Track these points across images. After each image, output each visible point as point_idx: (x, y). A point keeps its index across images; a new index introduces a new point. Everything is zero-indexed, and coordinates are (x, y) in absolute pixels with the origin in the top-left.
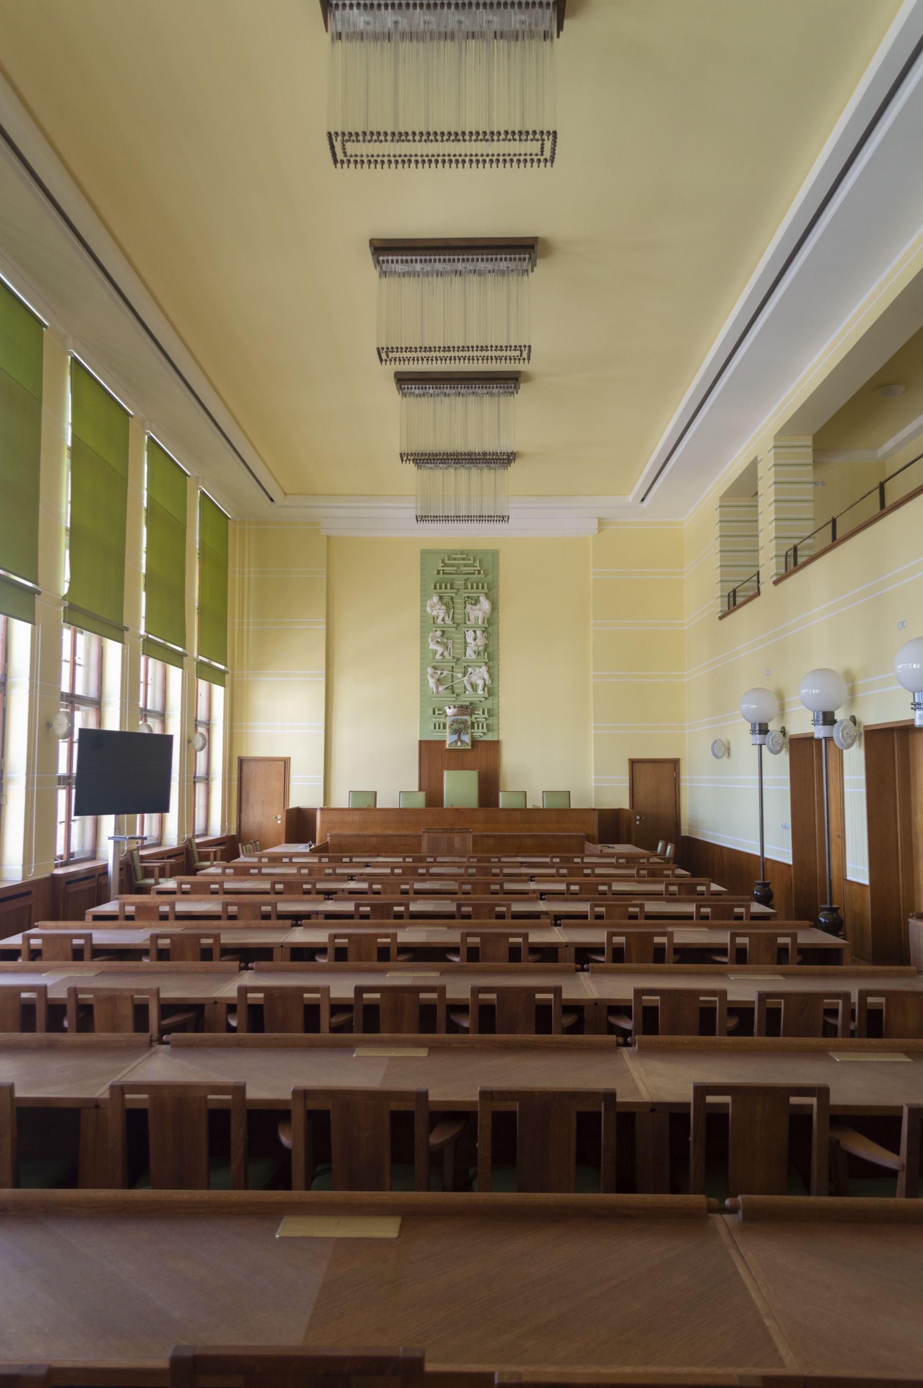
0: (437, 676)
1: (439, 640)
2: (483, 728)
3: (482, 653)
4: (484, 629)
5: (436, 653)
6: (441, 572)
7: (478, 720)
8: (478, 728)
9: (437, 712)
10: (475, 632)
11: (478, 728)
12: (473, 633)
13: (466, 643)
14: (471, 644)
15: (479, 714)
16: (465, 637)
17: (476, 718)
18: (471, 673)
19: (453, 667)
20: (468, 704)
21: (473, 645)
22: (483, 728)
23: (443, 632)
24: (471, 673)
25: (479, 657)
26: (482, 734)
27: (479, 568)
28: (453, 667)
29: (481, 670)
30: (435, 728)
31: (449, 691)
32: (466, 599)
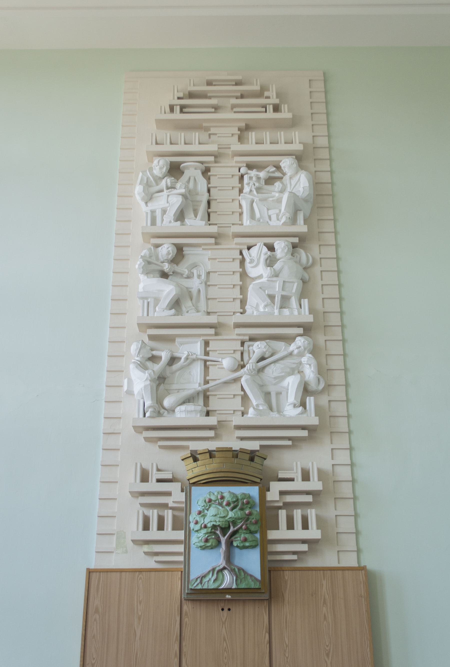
0: (157, 367)
1: (166, 267)
2: (305, 526)
3: (294, 302)
4: (296, 240)
5: (157, 301)
6: (178, 109)
7: (289, 499)
8: (290, 526)
9: (154, 475)
10: (271, 248)
11: (290, 526)
12: (265, 249)
13: (244, 275)
14: (260, 277)
15: (292, 480)
16: (242, 262)
17: (282, 493)
18: (262, 359)
19: (207, 344)
20: (254, 446)
21: (264, 280)
22: (305, 526)
23: (180, 249)
24: (262, 359)
25: (286, 312)
26: (305, 547)
27: (277, 101)
28: (207, 344)
29: (293, 347)
30: (146, 527)
31: (199, 406)
32: (243, 170)
